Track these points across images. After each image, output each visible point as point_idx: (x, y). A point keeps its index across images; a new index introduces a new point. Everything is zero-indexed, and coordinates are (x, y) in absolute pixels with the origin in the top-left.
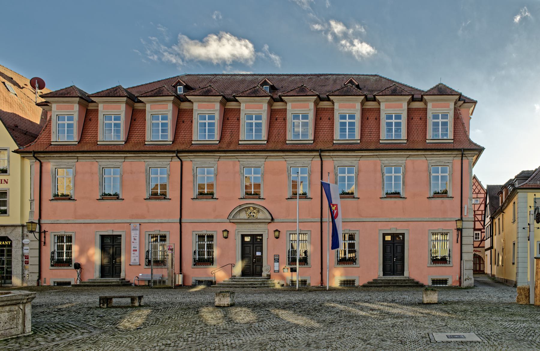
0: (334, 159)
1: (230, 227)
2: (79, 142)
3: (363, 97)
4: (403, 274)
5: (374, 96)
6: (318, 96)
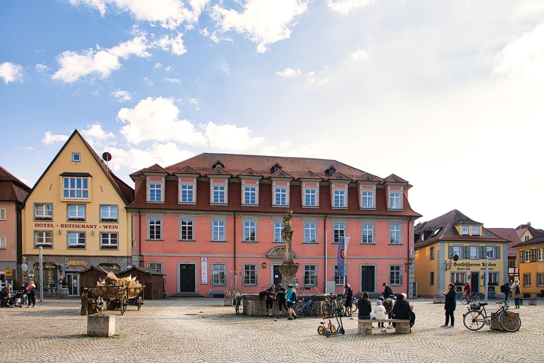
1: (266, 261)
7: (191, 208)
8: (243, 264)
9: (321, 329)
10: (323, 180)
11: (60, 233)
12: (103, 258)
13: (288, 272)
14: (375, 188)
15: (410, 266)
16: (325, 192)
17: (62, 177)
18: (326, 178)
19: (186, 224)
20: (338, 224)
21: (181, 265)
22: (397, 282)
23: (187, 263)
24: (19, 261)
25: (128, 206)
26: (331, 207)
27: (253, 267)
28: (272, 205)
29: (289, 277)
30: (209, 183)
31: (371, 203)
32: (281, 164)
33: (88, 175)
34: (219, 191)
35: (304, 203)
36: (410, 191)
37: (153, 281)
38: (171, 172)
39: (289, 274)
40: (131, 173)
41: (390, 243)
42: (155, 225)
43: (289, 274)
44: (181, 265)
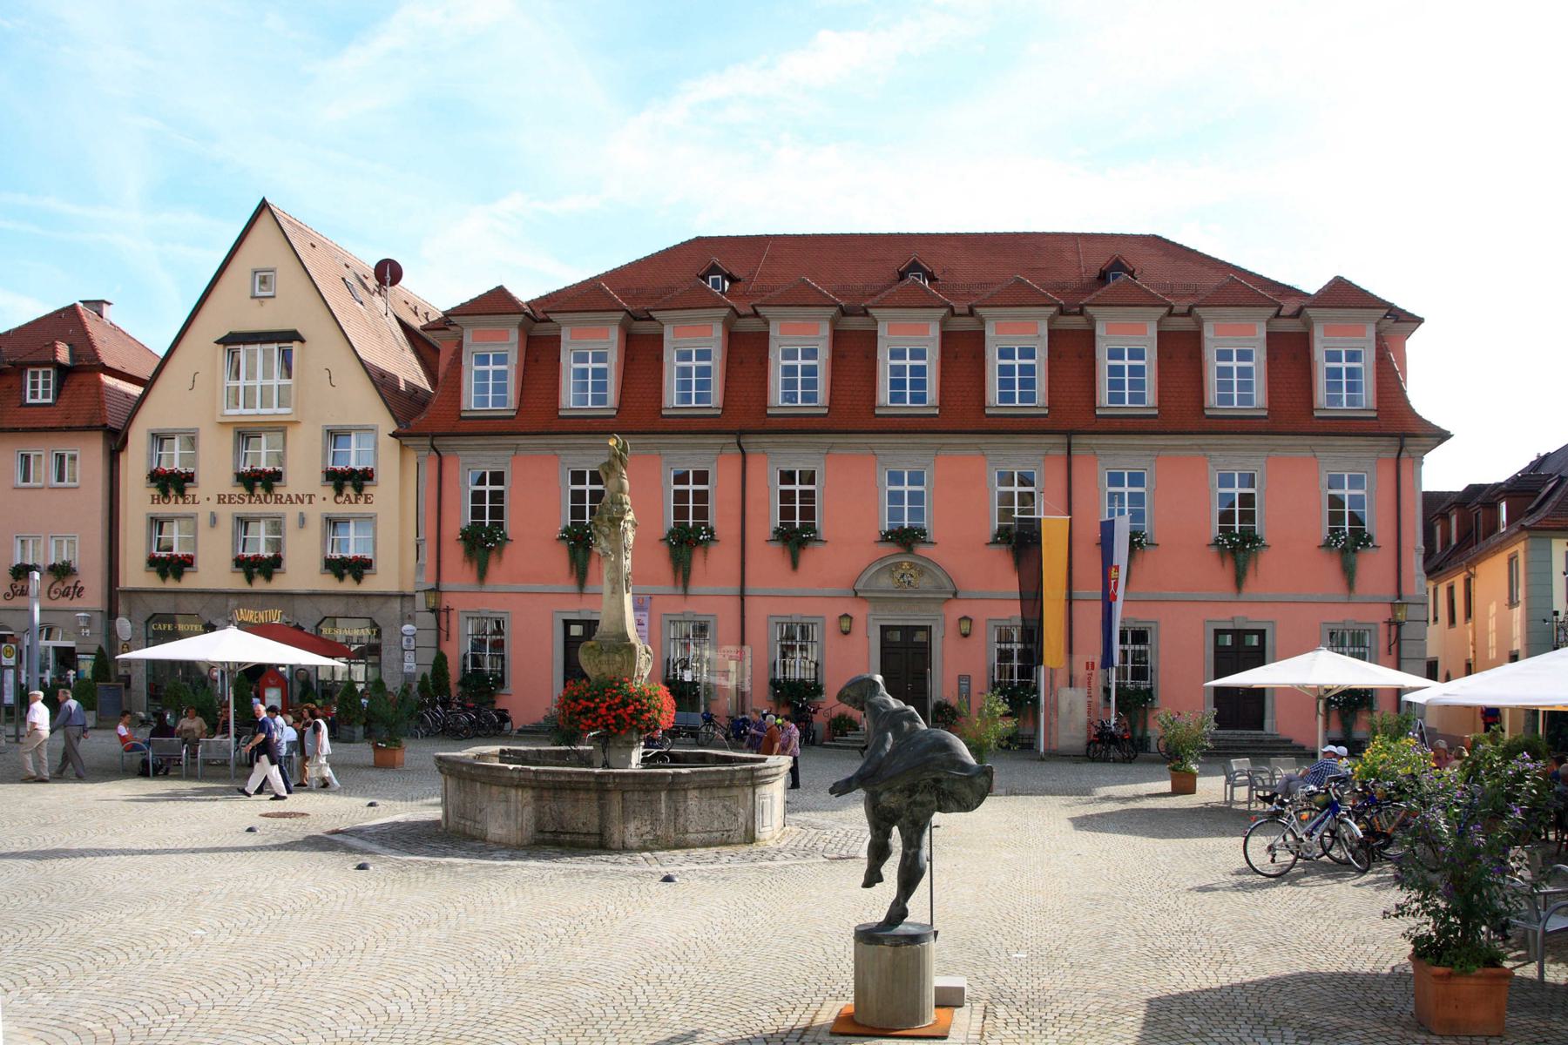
2: (518, 410)
3: (945, 311)
4: (1261, 727)
5: (1082, 307)
6: (1061, 307)
11: (214, 520)
12: (332, 600)
17: (221, 347)
24: (111, 614)
28: (1203, 409)
33: (293, 336)
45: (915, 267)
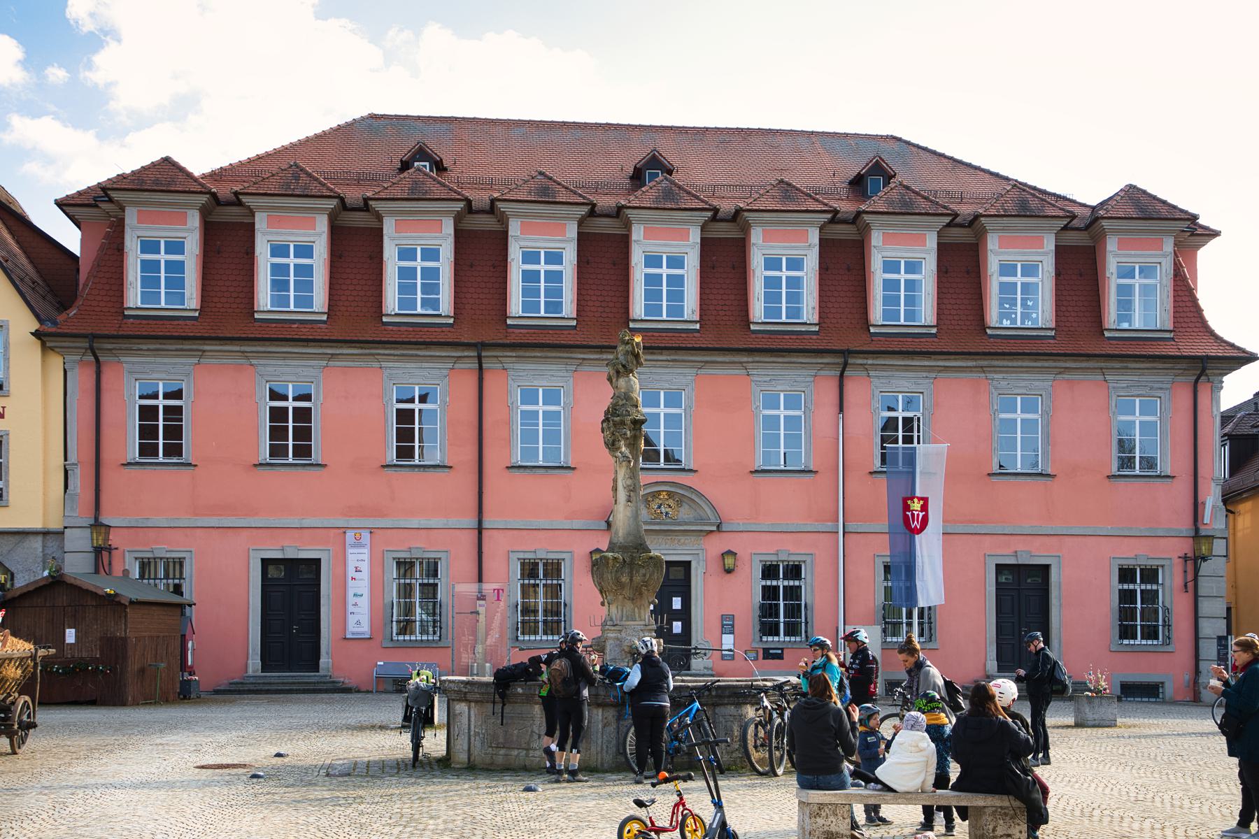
0: (872, 373)
7: (305, 333)
8: (514, 557)
9: (635, 827)
10: (836, 217)
13: (621, 586)
14: (1049, 243)
15: (1205, 568)
16: (844, 261)
18: (846, 207)
19: (285, 398)
20: (880, 393)
21: (265, 563)
22: (1151, 633)
23: (291, 554)
25: (49, 328)
26: (866, 324)
27: (554, 569)
29: (629, 605)
30: (378, 235)
31: (1035, 307)
32: (671, 156)
34: (418, 265)
35: (758, 310)
36: (1206, 256)
37: (135, 628)
38: (224, 191)
39: (627, 592)
40: (61, 195)
41: (1114, 470)
42: (161, 403)
43: (627, 592)
44: (265, 563)
45: (421, 153)
